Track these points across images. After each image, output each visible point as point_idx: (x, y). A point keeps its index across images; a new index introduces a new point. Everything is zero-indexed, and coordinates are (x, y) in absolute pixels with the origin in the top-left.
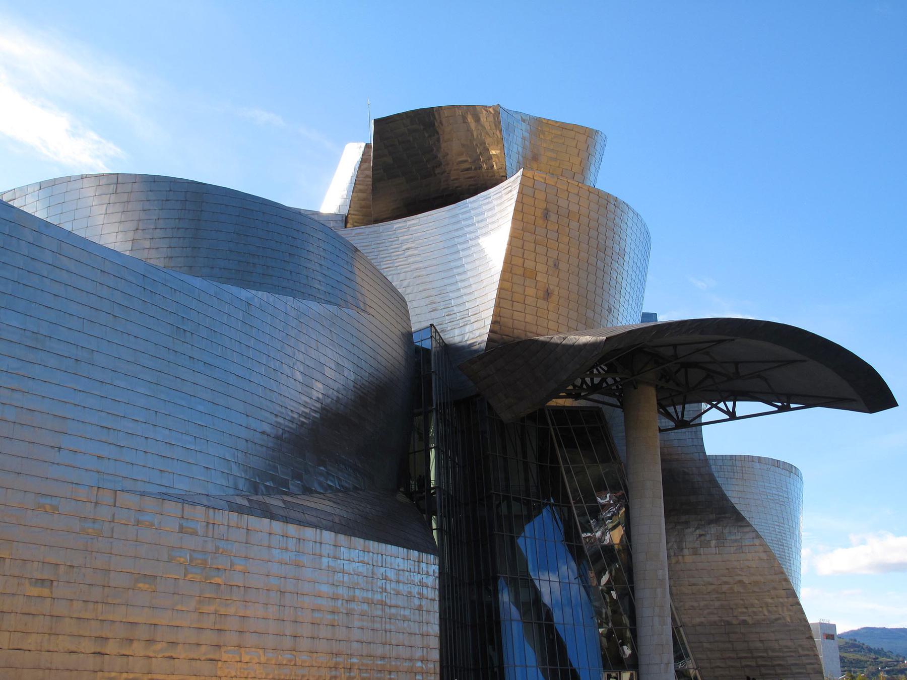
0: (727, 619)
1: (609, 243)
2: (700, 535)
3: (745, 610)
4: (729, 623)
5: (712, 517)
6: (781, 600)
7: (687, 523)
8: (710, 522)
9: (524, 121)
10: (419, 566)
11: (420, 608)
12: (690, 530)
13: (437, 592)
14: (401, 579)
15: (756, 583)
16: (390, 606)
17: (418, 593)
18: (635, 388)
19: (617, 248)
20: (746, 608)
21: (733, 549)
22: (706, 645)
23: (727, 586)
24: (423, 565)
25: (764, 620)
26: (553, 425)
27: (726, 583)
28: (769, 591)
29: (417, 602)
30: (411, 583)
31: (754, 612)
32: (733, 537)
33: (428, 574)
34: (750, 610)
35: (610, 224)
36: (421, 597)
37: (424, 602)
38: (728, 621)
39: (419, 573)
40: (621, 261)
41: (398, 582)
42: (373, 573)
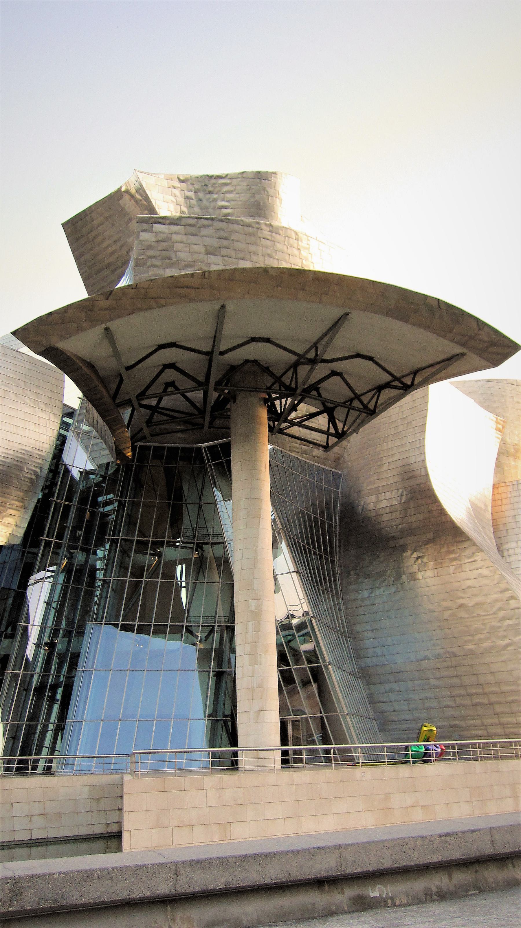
0: (454, 650)
2: (418, 558)
3: (470, 638)
4: (455, 655)
5: (430, 536)
6: (510, 622)
7: (403, 548)
8: (428, 542)
12: (409, 553)
15: (479, 605)
20: (472, 635)
21: (452, 569)
22: (433, 682)
23: (449, 612)
25: (493, 647)
26: (209, 462)
27: (447, 609)
28: (495, 613)
31: (480, 639)
32: (452, 556)
34: (477, 637)
38: (453, 653)
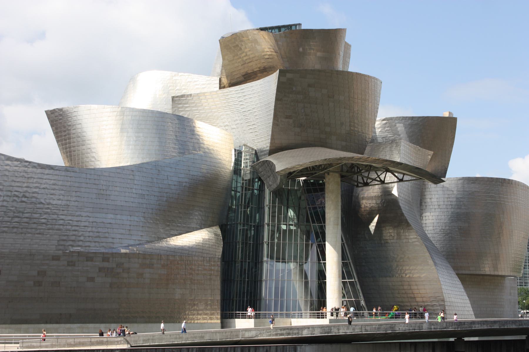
13: (219, 273)
36: (211, 275)
42: (186, 268)
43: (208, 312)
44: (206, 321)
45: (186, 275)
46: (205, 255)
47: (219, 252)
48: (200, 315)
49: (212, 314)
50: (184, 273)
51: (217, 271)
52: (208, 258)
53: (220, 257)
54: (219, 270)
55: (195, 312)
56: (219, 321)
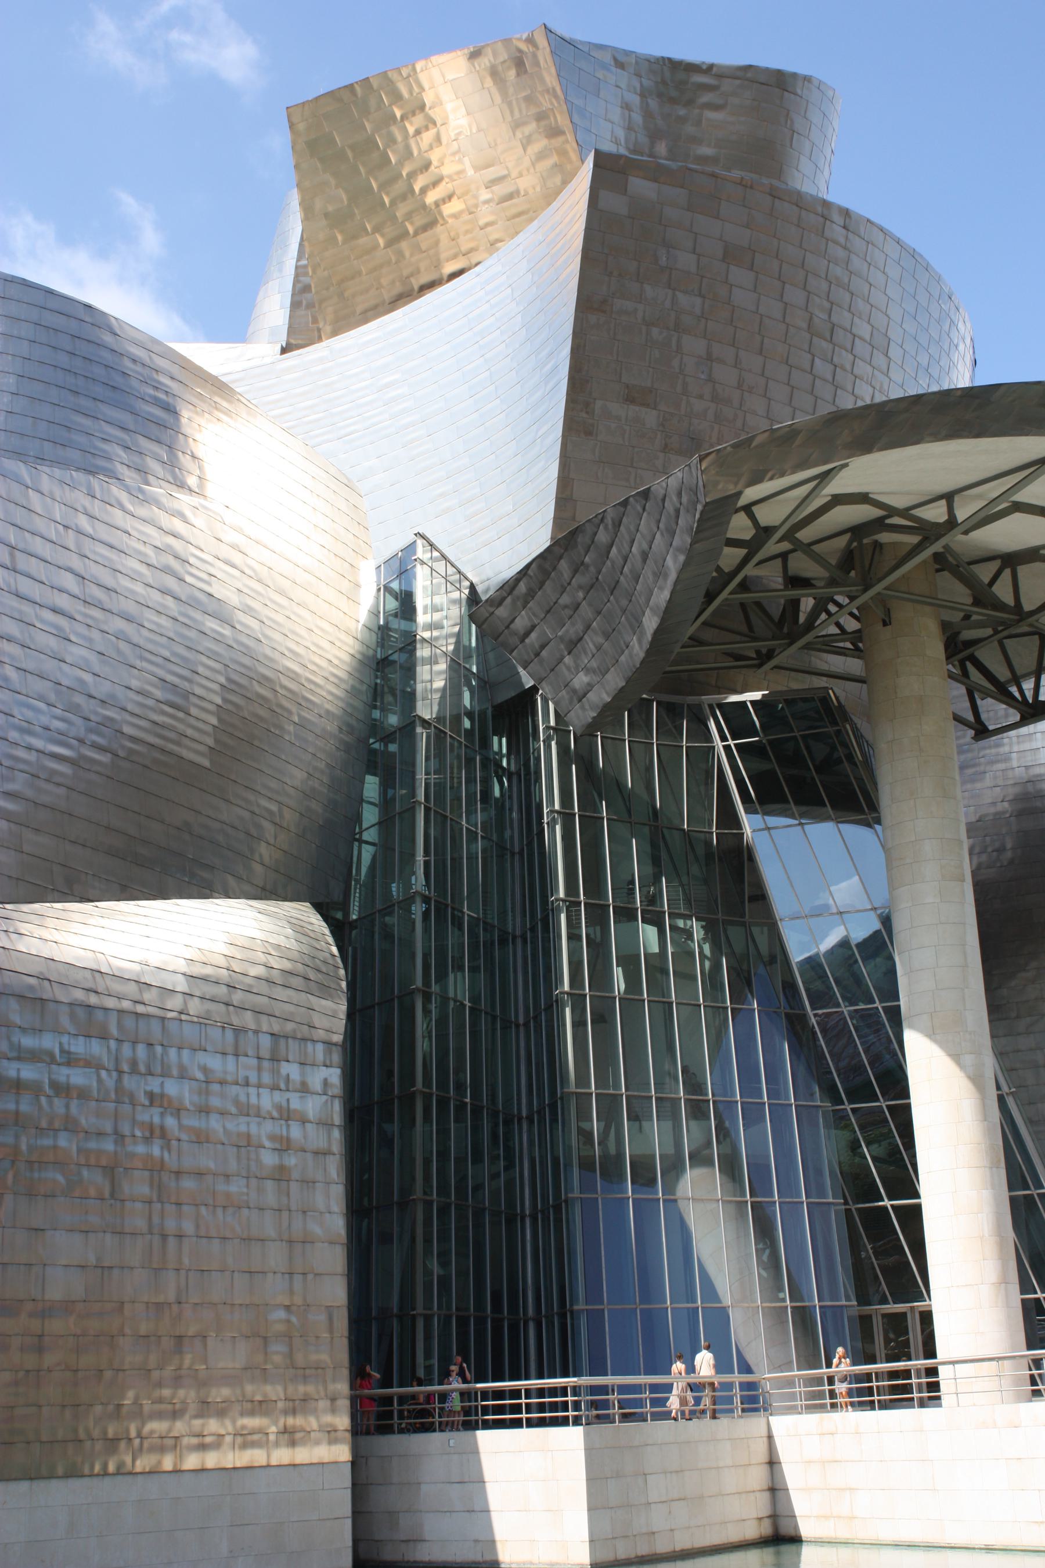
1: (842, 317)
9: (620, 65)
10: (275, 1072)
11: (281, 1175)
13: (337, 1134)
14: (215, 1102)
16: (178, 1173)
17: (272, 1138)
18: (885, 624)
19: (863, 330)
24: (291, 1070)
26: (723, 738)
29: (269, 1159)
30: (246, 1110)
33: (304, 1089)
35: (837, 271)
36: (284, 1145)
37: (291, 1160)
39: (275, 1088)
40: (879, 360)
41: (204, 1110)
42: (119, 1088)
43: (274, 1391)
44: (256, 1456)
45: (119, 1137)
46: (248, 1020)
47: (331, 1015)
48: (221, 1413)
49: (298, 1405)
50: (108, 1127)
51: (325, 1124)
52: (266, 1041)
53: (338, 1038)
54: (338, 1118)
55: (187, 1394)
56: (343, 1453)
